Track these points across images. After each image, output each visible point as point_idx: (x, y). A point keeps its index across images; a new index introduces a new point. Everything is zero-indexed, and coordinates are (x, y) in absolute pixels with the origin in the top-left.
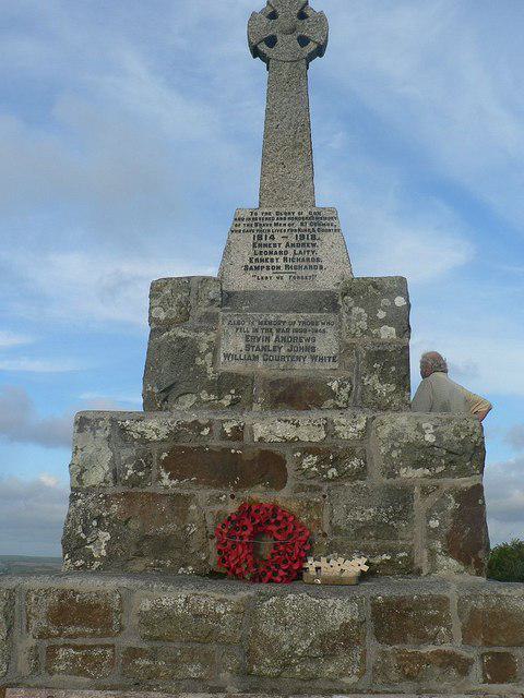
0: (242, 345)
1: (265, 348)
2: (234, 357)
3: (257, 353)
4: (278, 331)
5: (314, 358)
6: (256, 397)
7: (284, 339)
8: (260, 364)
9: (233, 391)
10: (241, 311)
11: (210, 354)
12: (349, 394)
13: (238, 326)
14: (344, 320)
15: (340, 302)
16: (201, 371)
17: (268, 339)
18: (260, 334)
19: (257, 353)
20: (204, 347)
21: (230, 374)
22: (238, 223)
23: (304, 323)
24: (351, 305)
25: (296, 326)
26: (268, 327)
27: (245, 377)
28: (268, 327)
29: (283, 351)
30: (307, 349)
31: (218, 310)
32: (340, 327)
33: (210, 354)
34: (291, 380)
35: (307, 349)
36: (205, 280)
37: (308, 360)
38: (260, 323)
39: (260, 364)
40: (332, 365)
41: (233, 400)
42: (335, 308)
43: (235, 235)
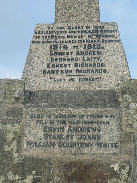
0: (41, 134)
1: (60, 137)
2: (35, 144)
3: (53, 141)
4: (70, 122)
5: (99, 145)
6: (53, 176)
7: (75, 129)
8: (56, 149)
9: (34, 172)
10: (41, 107)
11: (15, 143)
12: (129, 173)
13: (37, 119)
14: (124, 113)
15: (120, 99)
16: (8, 156)
17: (62, 129)
18: (56, 125)
19: (53, 141)
20: (10, 136)
21: (32, 158)
22: (38, 35)
23: (91, 116)
24: (128, 101)
25: (85, 119)
26: (63, 119)
27: (44, 160)
28: (63, 119)
29: (75, 139)
30: (94, 137)
31: (22, 106)
32: (120, 119)
33: (15, 143)
34: (82, 163)
35: (94, 137)
36: (11, 82)
37: (95, 146)
38: (56, 117)
39: (56, 149)
40: (113, 150)
41: (34, 179)
42: (116, 103)
43: (36, 45)
